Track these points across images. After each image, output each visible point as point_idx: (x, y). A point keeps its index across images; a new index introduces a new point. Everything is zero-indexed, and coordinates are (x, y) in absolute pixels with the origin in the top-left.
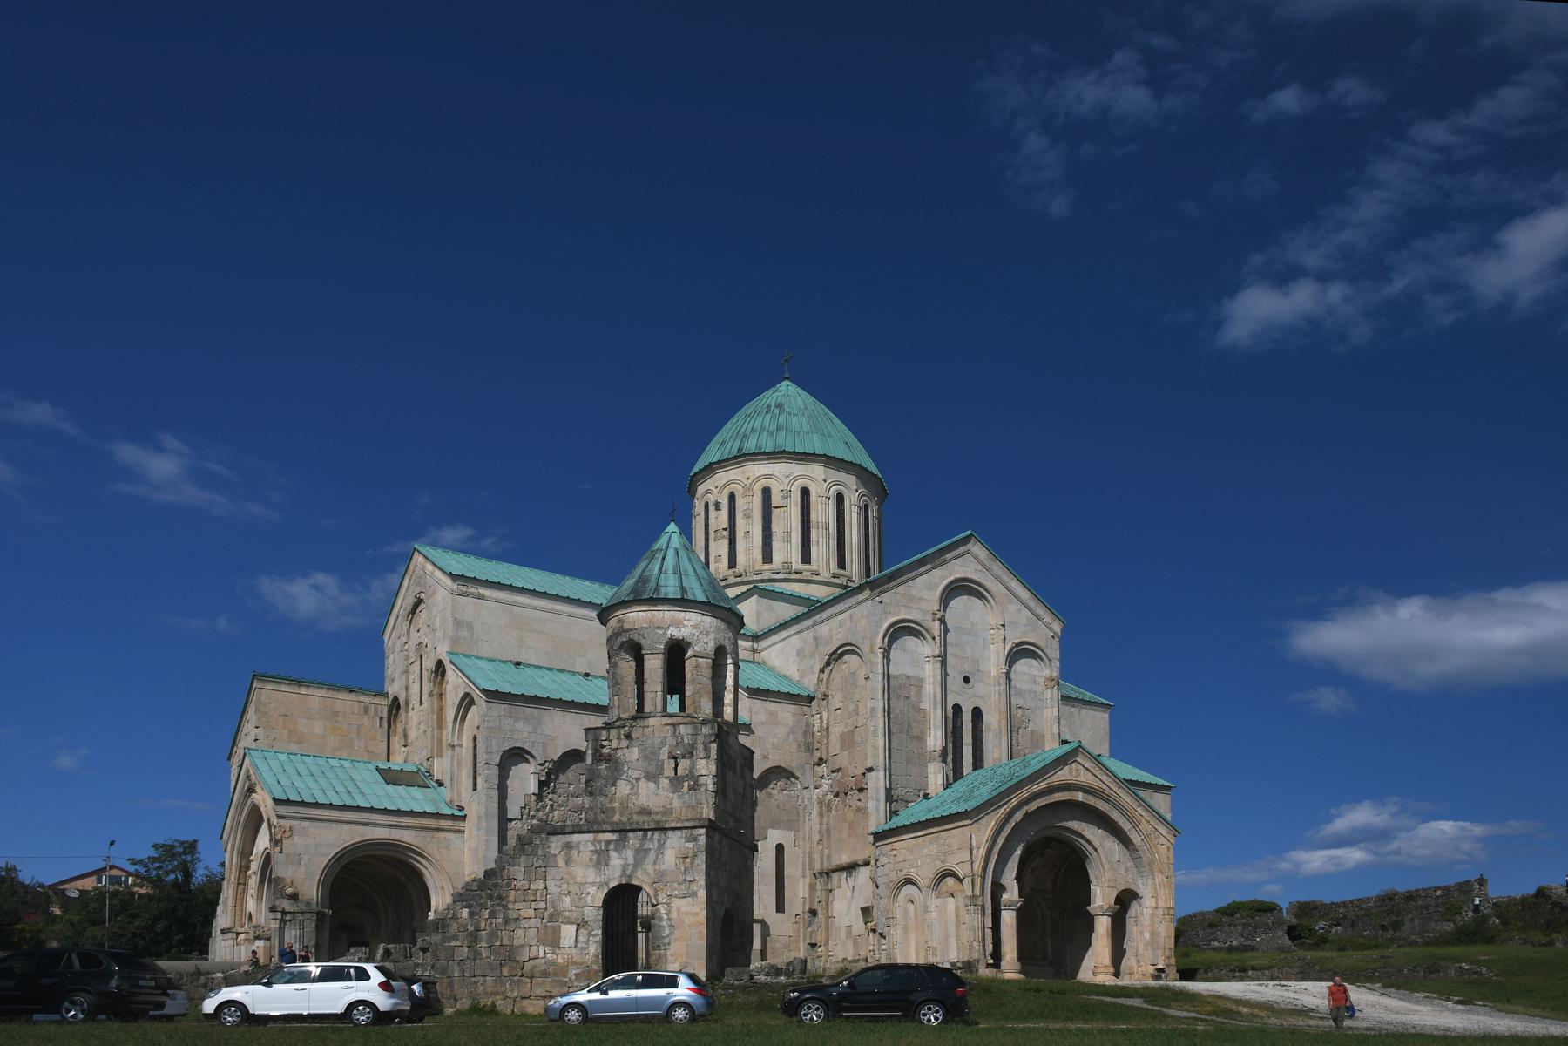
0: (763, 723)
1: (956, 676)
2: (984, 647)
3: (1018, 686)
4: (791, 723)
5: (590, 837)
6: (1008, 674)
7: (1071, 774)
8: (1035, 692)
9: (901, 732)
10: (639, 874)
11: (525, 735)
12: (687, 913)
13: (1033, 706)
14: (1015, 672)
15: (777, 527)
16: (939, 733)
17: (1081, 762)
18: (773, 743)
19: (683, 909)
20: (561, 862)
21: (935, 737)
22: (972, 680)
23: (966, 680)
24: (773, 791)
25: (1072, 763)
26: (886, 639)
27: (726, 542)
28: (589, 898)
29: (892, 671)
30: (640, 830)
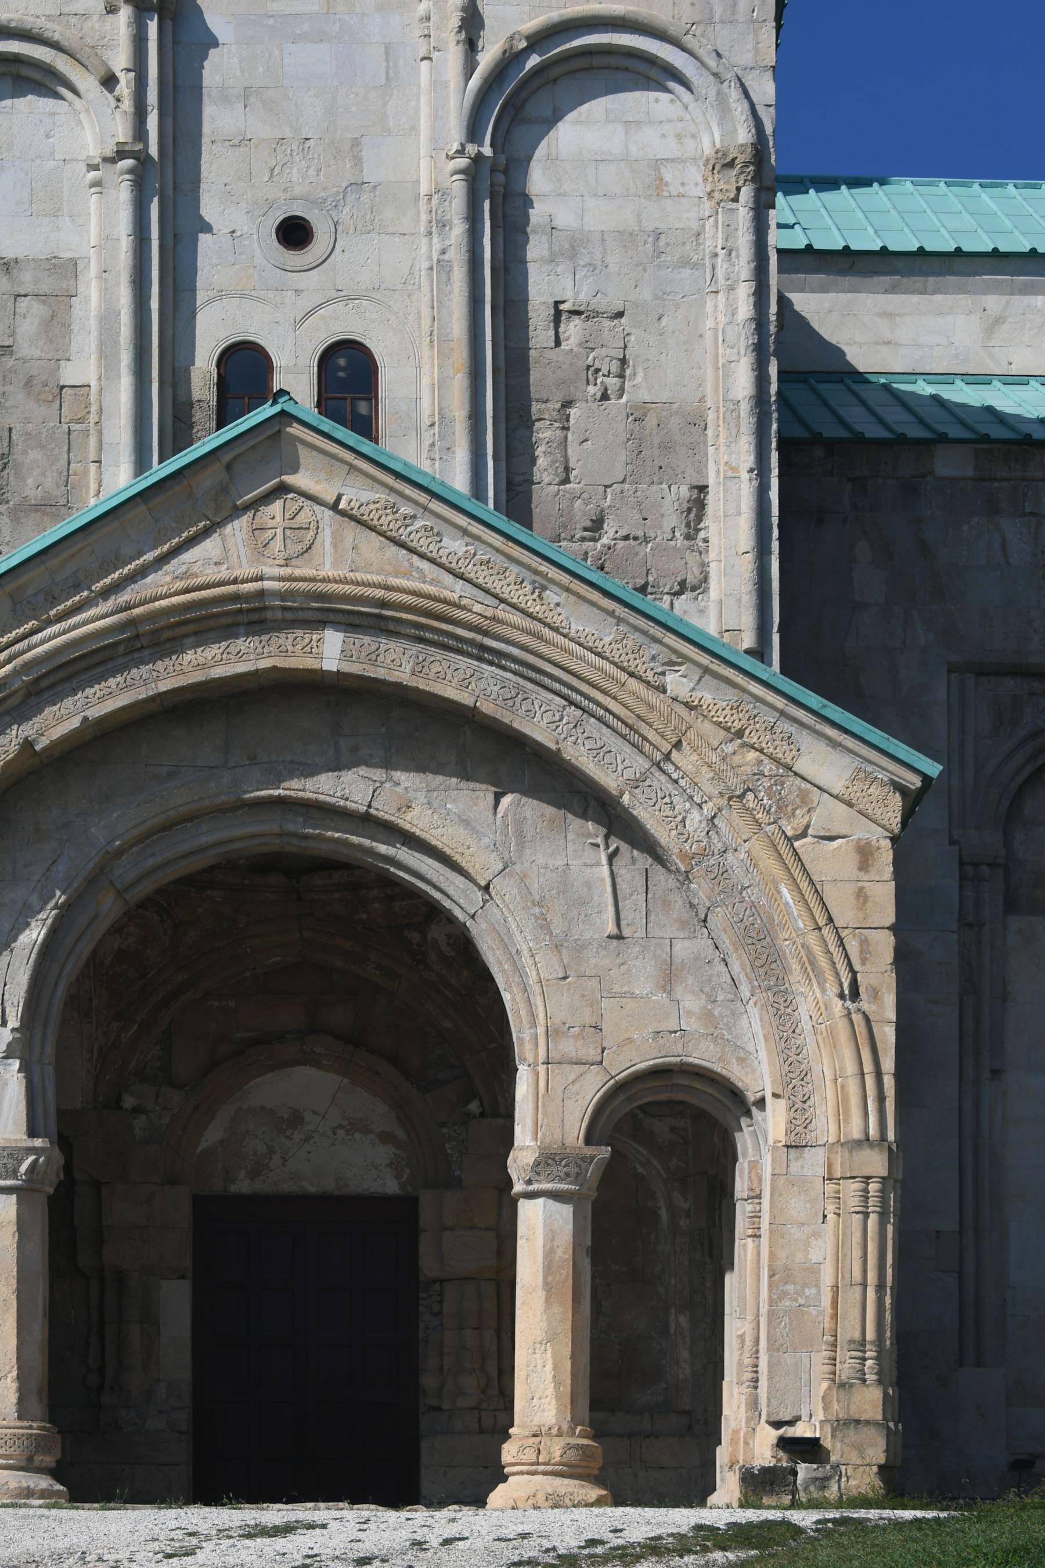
3: (565, 218)
8: (658, 235)
13: (646, 294)
14: (552, 159)
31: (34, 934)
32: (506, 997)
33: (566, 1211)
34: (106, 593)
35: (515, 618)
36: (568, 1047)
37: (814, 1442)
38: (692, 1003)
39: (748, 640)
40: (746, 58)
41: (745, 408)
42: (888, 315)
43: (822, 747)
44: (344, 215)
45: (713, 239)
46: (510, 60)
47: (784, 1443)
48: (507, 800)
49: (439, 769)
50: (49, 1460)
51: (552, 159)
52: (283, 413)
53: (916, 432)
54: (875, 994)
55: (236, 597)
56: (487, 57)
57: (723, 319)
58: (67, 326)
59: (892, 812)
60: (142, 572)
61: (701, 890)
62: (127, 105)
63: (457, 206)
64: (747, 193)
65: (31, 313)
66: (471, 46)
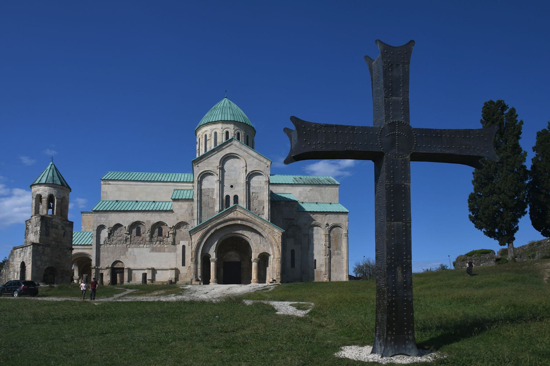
0: (177, 209)
1: (228, 186)
3: (253, 185)
4: (187, 208)
6: (248, 184)
7: (234, 215)
8: (261, 187)
9: (205, 206)
14: (252, 181)
16: (218, 205)
17: (238, 210)
21: (217, 208)
22: (233, 188)
23: (232, 186)
24: (182, 229)
25: (235, 211)
26: (199, 178)
27: (198, 153)
29: (203, 187)
31: (216, 243)
32: (251, 247)
33: (256, 263)
34: (222, 218)
36: (256, 251)
37: (275, 280)
38: (266, 248)
39: (268, 218)
40: (268, 173)
42: (276, 188)
44: (236, 185)
45: (265, 187)
46: (249, 173)
50: (217, 282)
51: (252, 181)
52: (236, 205)
53: (279, 200)
54: (280, 247)
56: (247, 173)
58: (214, 194)
59: (281, 234)
60: (225, 216)
61: (267, 240)
62: (219, 177)
63: (245, 185)
64: (268, 184)
66: (246, 172)
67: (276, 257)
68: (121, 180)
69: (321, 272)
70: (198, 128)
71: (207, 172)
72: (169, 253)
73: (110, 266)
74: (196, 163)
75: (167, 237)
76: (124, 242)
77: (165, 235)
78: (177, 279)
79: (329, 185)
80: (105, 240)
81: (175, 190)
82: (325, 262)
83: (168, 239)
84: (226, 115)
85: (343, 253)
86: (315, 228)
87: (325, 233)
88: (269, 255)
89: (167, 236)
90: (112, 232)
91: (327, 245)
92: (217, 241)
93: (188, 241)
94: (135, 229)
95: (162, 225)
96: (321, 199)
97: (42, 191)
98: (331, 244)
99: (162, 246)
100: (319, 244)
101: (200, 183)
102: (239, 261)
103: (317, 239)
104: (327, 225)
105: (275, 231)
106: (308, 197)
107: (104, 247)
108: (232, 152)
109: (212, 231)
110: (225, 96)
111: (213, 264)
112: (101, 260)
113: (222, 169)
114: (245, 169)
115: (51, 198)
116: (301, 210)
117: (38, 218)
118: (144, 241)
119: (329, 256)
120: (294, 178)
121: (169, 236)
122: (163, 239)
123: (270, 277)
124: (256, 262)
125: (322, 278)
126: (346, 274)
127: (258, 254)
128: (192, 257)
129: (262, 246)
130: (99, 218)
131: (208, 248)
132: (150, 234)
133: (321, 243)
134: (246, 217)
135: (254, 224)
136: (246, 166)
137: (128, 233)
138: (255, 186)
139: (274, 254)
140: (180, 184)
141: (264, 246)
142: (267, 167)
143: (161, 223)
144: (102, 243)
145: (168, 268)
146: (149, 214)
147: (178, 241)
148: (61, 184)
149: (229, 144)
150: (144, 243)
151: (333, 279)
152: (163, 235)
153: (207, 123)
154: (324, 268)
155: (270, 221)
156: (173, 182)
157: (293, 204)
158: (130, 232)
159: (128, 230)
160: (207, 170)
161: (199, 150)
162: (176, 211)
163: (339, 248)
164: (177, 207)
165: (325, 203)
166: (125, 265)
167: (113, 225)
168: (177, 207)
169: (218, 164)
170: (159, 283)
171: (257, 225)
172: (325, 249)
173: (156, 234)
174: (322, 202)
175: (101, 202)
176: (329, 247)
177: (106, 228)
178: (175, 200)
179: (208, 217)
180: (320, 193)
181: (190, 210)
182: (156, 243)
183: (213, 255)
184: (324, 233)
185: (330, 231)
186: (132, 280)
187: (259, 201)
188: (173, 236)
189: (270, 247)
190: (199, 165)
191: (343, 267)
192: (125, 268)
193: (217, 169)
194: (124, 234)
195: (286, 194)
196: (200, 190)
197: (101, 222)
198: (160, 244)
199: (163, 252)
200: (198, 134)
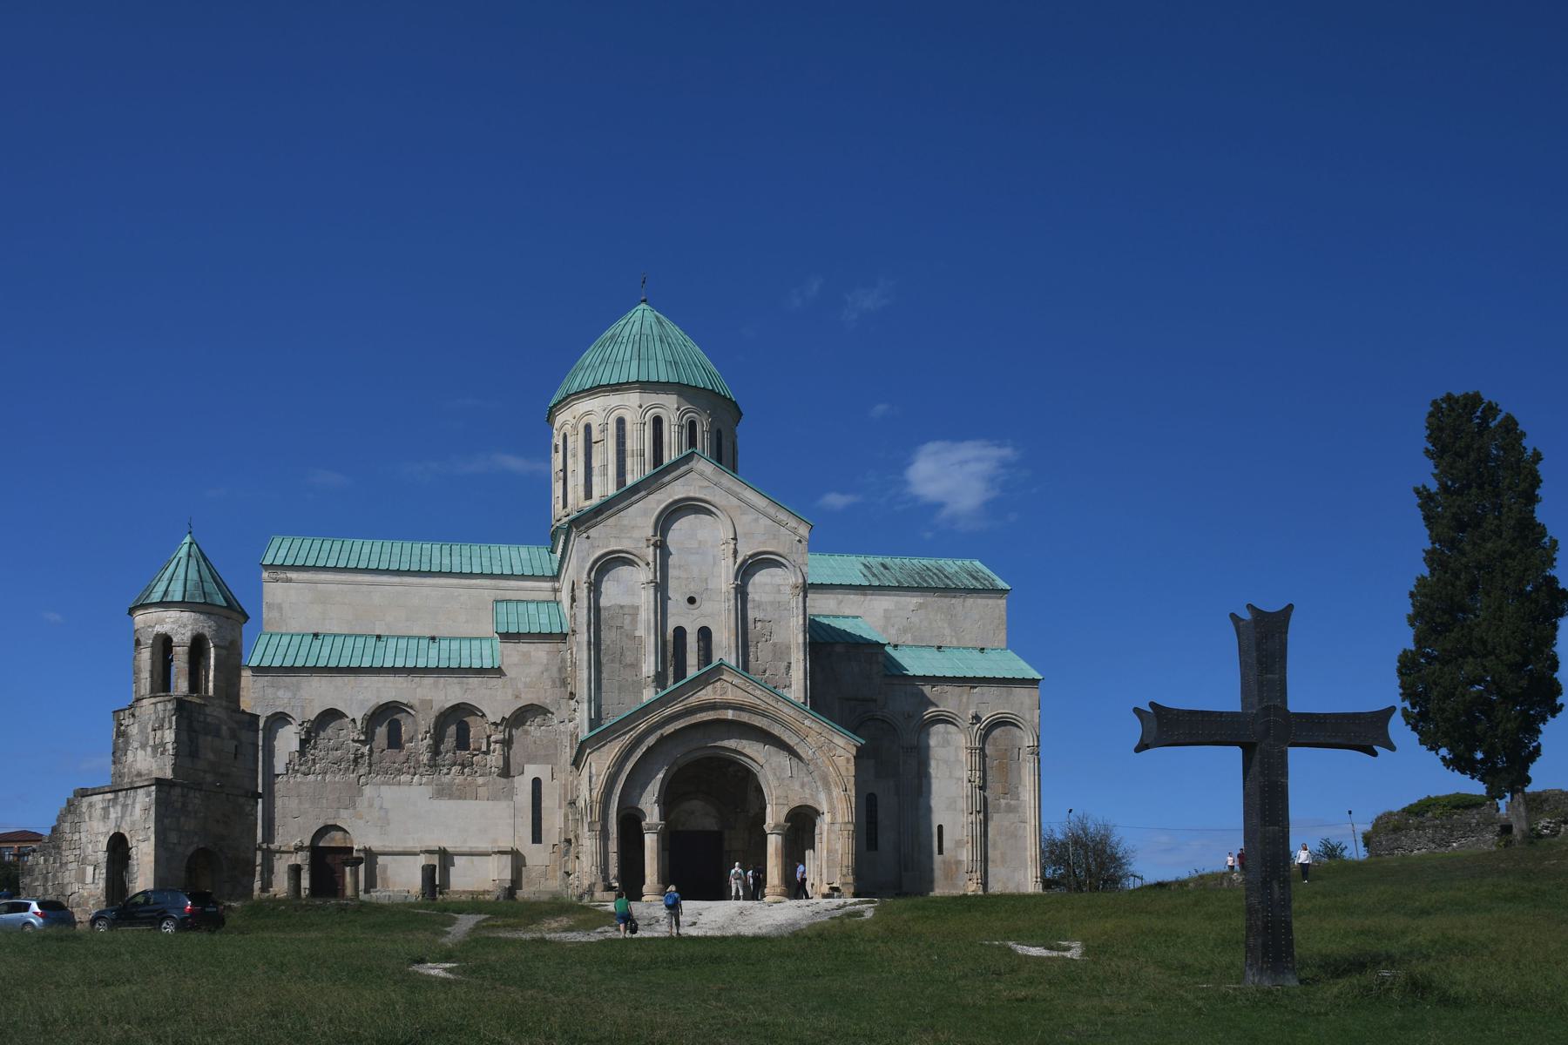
0: (515, 665)
2: (715, 564)
3: (757, 598)
4: (545, 661)
5: (100, 797)
6: (741, 592)
7: (715, 693)
8: (779, 602)
9: (613, 661)
10: (124, 823)
11: (286, 701)
12: (146, 853)
14: (754, 584)
15: (596, 463)
16: (653, 658)
18: (525, 683)
19: (144, 851)
20: (87, 819)
21: (649, 666)
22: (698, 600)
24: (529, 728)
26: (593, 574)
27: (561, 482)
28: (100, 845)
29: (603, 602)
30: (124, 790)
31: (660, 776)
34: (680, 702)
35: (771, 708)
36: (781, 801)
37: (838, 888)
38: (807, 791)
39: (802, 700)
41: (801, 645)
43: (839, 737)
46: (745, 561)
47: (831, 888)
48: (767, 746)
49: (751, 740)
54: (850, 791)
55: (710, 703)
56: (739, 561)
57: (795, 624)
60: (689, 697)
61: (811, 768)
62: (652, 570)
63: (732, 596)
64: (801, 594)
65: (628, 619)
66: (735, 557)
67: (840, 820)
68: (325, 569)
69: (959, 863)
70: (560, 402)
71: (616, 555)
72: (491, 802)
73: (307, 843)
74: (582, 528)
75: (484, 753)
76: (349, 769)
77: (477, 746)
78: (516, 882)
79: (975, 591)
80: (290, 761)
81: (497, 601)
82: (970, 834)
83: (488, 757)
84: (652, 363)
85: (1025, 807)
86: (940, 727)
87: (969, 745)
88: (817, 813)
89: (484, 748)
90: (313, 735)
91: (977, 780)
92: (663, 771)
93: (549, 764)
94: (385, 724)
95: (469, 716)
96: (953, 634)
97: (173, 626)
98: (989, 778)
99: (469, 779)
100: (950, 777)
101: (595, 588)
102: (716, 829)
103: (946, 762)
104: (977, 718)
105: (835, 741)
106: (910, 629)
107: (288, 782)
108: (692, 495)
109: (651, 740)
110: (643, 298)
111: (652, 841)
112: (277, 824)
113: (662, 547)
114: (732, 546)
115: (197, 646)
116: (894, 672)
117: (165, 705)
118: (412, 764)
119: (981, 816)
120: (865, 565)
121: (492, 748)
122: (472, 758)
123: (821, 880)
124: (778, 834)
125: (961, 884)
126: (1034, 870)
127: (786, 811)
128: (591, 817)
129: (797, 787)
130: (269, 691)
131: (638, 791)
132: (431, 742)
133: (958, 774)
134: (749, 700)
135: (775, 720)
136: (735, 539)
137: (362, 738)
138: (763, 600)
139: (832, 811)
140: (513, 583)
141: (803, 785)
142: (800, 541)
143: (464, 709)
144: (279, 768)
145: (490, 850)
146: (428, 680)
147: (519, 764)
148: (225, 605)
149: (683, 469)
150: (412, 770)
151: (995, 887)
152: (472, 747)
153: (591, 389)
154: (967, 852)
155: (808, 708)
156: (492, 576)
157: (869, 653)
158: (370, 735)
159: (362, 728)
160: (615, 548)
161: (565, 470)
162: (511, 673)
163: (1011, 791)
164: (515, 659)
165: (964, 648)
166: (355, 841)
167: (317, 714)
168: (515, 659)
169: (650, 532)
170: (463, 898)
171: (783, 724)
172: (970, 793)
173: (450, 741)
174: (955, 643)
175: (264, 639)
176: (983, 788)
177: (293, 722)
178: (506, 637)
179: (620, 693)
180: (950, 616)
181: (555, 670)
182: (450, 769)
183: (652, 812)
184: (966, 743)
185: (984, 738)
186: (376, 887)
187: (775, 645)
188: (503, 750)
189: (821, 789)
190: (593, 532)
191: (1026, 849)
192: (356, 847)
193: (648, 547)
194: (350, 742)
195: (844, 617)
196: (596, 610)
197: (277, 703)
198: (463, 773)
199: (471, 799)
200: (560, 419)
